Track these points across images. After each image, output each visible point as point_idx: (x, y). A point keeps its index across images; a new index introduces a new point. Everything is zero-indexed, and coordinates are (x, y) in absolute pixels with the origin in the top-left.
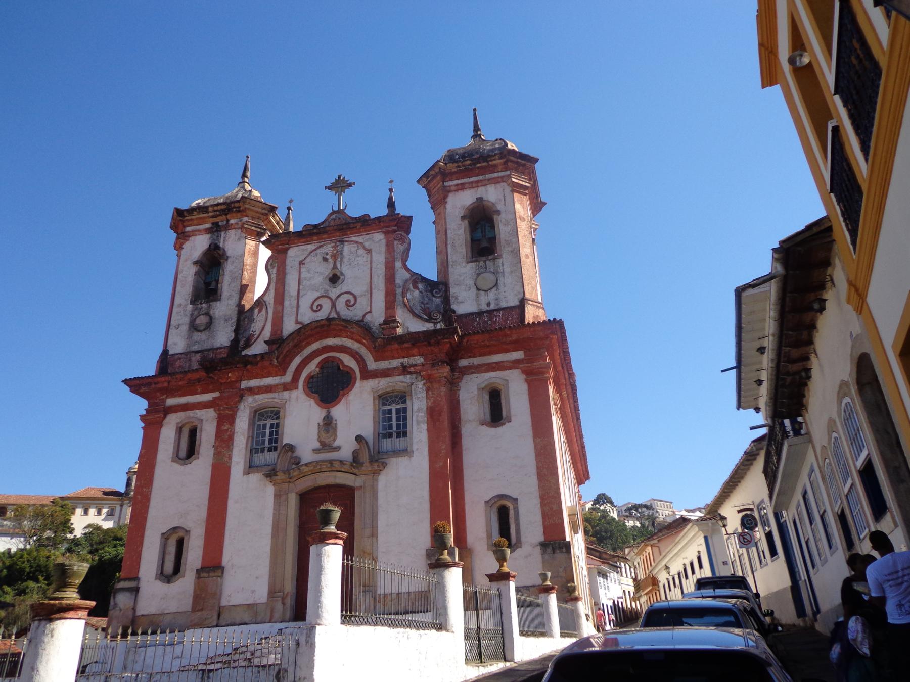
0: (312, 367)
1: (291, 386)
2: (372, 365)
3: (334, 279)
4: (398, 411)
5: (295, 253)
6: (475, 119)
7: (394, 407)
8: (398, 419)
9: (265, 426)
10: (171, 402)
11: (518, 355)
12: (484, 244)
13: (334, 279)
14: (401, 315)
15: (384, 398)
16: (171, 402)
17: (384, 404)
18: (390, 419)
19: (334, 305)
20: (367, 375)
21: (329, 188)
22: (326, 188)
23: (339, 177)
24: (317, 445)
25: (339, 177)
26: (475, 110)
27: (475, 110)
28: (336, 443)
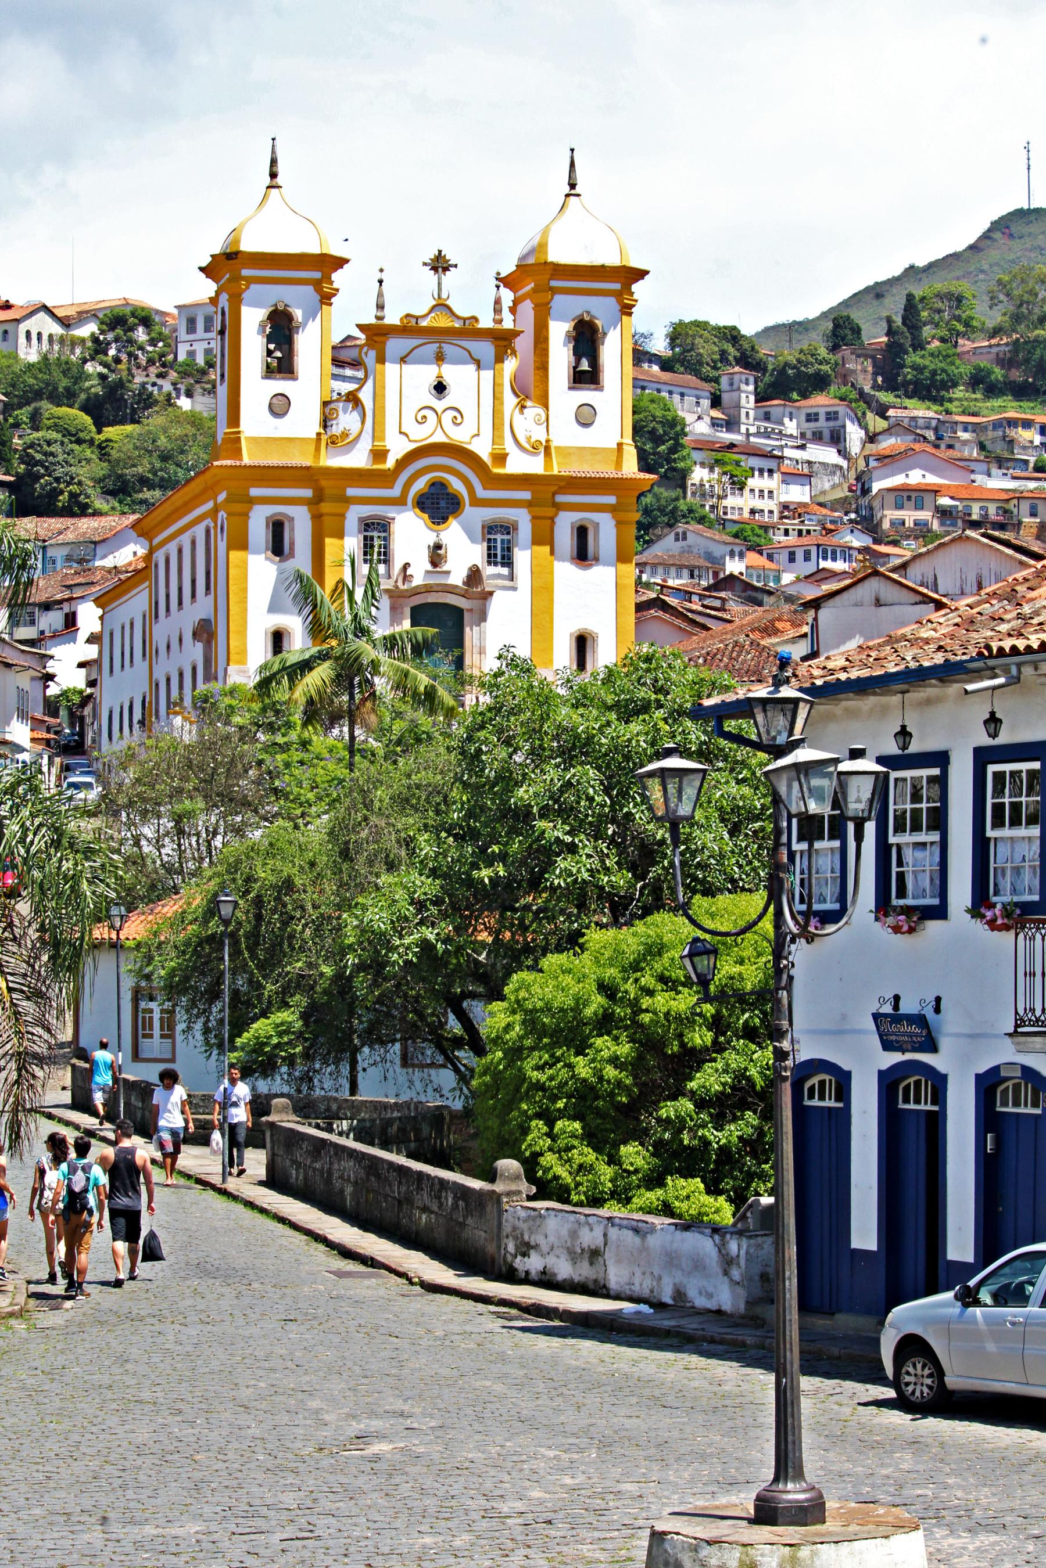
0: (421, 485)
1: (400, 502)
2: (481, 493)
3: (440, 388)
4: (503, 541)
5: (395, 345)
6: (572, 164)
7: (499, 537)
8: (503, 549)
9: (372, 539)
10: (254, 492)
11: (611, 500)
12: (585, 365)
13: (440, 388)
14: (509, 446)
15: (491, 529)
16: (254, 492)
17: (489, 533)
18: (495, 547)
19: (440, 421)
20: (476, 502)
21: (425, 264)
22: (425, 264)
23: (440, 252)
24: (429, 568)
25: (440, 252)
26: (572, 150)
27: (572, 150)
28: (445, 568)
